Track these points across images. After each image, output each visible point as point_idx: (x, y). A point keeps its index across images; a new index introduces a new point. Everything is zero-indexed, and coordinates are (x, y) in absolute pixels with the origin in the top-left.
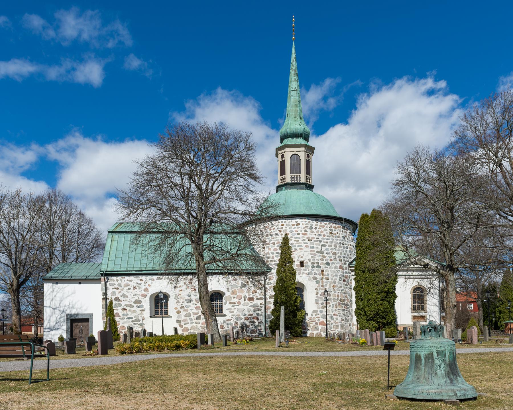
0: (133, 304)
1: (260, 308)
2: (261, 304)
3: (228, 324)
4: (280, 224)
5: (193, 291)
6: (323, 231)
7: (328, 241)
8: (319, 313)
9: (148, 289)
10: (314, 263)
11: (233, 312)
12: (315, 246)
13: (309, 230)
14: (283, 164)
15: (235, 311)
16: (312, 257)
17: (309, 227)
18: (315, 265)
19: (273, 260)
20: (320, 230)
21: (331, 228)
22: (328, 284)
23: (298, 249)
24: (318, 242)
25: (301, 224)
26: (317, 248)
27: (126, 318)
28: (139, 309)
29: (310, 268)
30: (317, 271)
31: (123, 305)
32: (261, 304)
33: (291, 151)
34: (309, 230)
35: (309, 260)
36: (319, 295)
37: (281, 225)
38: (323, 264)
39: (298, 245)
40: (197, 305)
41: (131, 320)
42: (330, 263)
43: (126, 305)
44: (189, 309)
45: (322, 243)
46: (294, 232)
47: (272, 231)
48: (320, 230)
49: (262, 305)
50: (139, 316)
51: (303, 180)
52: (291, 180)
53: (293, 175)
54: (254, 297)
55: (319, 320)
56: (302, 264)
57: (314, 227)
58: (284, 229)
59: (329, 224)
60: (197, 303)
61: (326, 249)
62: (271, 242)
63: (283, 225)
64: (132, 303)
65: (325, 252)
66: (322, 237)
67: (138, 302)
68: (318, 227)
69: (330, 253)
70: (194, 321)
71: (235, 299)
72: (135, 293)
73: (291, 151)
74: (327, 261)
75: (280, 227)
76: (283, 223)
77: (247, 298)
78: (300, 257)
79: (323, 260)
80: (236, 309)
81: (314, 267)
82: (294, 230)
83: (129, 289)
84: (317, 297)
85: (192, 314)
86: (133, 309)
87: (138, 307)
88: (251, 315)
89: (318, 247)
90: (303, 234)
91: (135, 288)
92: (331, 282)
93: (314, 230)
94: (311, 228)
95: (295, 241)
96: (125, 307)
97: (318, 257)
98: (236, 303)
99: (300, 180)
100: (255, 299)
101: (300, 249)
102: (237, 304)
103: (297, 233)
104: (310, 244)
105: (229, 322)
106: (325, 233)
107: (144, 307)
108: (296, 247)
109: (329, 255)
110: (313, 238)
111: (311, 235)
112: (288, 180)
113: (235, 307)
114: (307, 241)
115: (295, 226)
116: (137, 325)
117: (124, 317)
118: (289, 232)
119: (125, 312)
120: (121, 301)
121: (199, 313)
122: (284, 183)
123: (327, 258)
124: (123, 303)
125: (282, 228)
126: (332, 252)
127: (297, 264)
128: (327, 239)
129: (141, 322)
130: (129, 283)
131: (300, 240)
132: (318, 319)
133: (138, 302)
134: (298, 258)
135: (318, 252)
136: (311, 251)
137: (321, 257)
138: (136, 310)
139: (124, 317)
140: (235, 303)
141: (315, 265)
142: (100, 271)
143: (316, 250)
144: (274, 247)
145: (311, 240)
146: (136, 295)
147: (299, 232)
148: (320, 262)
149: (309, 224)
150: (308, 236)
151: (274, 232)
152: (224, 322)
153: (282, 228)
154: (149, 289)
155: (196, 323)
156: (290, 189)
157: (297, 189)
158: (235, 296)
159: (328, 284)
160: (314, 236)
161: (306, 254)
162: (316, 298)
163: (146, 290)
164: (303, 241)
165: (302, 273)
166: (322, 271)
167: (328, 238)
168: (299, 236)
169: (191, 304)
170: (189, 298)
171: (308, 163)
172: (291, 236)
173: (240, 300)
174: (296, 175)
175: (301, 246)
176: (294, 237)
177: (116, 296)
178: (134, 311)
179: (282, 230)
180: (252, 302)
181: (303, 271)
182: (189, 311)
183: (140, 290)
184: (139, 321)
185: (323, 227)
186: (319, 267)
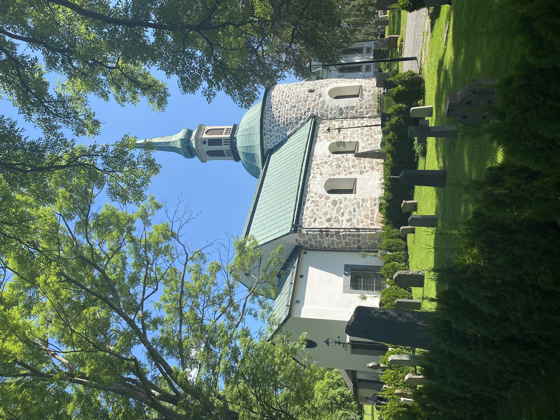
19: (303, 113)
27: (353, 213)
33: (203, 135)
41: (357, 209)
43: (338, 212)
44: (347, 166)
64: (335, 208)
72: (323, 204)
76: (269, 107)
82: (278, 99)
96: (340, 213)
116: (364, 205)
120: (332, 217)
124: (334, 215)
125: (274, 108)
129: (361, 202)
154: (319, 193)
163: (321, 197)
168: (284, 95)
170: (334, 167)
177: (325, 221)
182: (351, 166)
184: (358, 203)
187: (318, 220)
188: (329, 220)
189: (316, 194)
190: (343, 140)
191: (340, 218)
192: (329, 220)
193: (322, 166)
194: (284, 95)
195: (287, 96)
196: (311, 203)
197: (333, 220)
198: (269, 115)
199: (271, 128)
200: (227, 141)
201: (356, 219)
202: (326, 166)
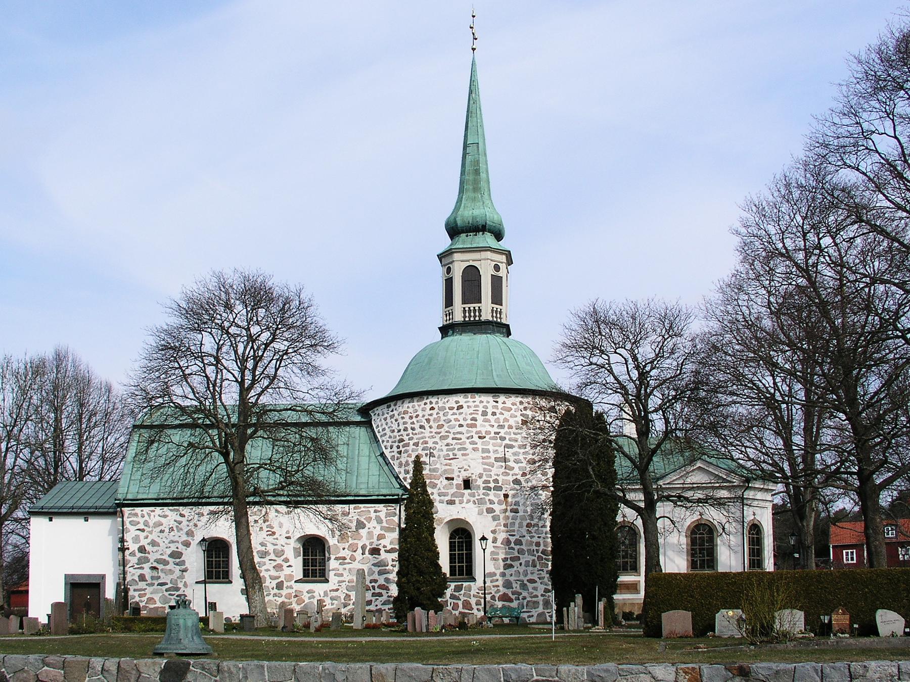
0: (168, 559)
1: (391, 568)
2: (393, 560)
3: (332, 599)
4: (428, 406)
5: (270, 535)
6: (507, 417)
7: (518, 437)
8: (498, 577)
9: (193, 532)
10: (489, 482)
11: (342, 575)
12: (491, 448)
13: (480, 418)
14: (449, 283)
15: (346, 573)
16: (485, 470)
17: (480, 413)
18: (492, 485)
20: (502, 418)
21: (524, 412)
22: (517, 522)
23: (459, 453)
24: (499, 441)
25: (465, 406)
26: (496, 451)
28: (178, 568)
29: (481, 491)
30: (495, 495)
31: (152, 561)
32: (393, 560)
34: (480, 418)
35: (481, 476)
36: (499, 544)
37: (430, 410)
38: (506, 482)
39: (460, 446)
40: (277, 563)
42: (522, 479)
43: (157, 561)
45: (507, 442)
46: (453, 422)
47: (414, 420)
48: (502, 418)
49: (394, 563)
50: (179, 581)
51: (486, 316)
52: (465, 317)
54: (380, 547)
55: (498, 591)
56: (467, 484)
57: (490, 411)
58: (435, 416)
59: (521, 403)
60: (276, 558)
61: (515, 454)
62: (411, 442)
63: (432, 409)
64: (166, 557)
65: (512, 458)
66: (506, 429)
67: (176, 555)
68: (498, 412)
69: (523, 460)
70: (273, 592)
71: (346, 550)
74: (515, 477)
75: (428, 412)
77: (368, 548)
78: (462, 470)
79: (508, 474)
80: (347, 571)
81: (489, 489)
82: (452, 418)
83: (162, 531)
84: (494, 547)
85: (268, 578)
86: (168, 567)
87: (177, 564)
88: (376, 581)
89: (497, 450)
90: (468, 425)
91: (171, 529)
92: (523, 518)
93: (489, 416)
94: (484, 413)
95: (453, 439)
96: (155, 564)
97: (497, 470)
98: (348, 558)
99: (480, 316)
100: (382, 552)
101: (463, 455)
102: (348, 561)
103: (458, 423)
104: (483, 443)
105: (334, 594)
106: (512, 422)
107: (187, 565)
108: (456, 452)
109: (520, 465)
110: (488, 433)
111: (484, 426)
112: (458, 317)
113: (345, 566)
114: (476, 439)
115: (455, 411)
116: (175, 597)
117: (153, 582)
118: (443, 423)
119: (155, 574)
120: (149, 553)
121: (280, 577)
122: (451, 321)
123: (516, 470)
124: (152, 557)
125: (431, 415)
126: (525, 458)
127: (456, 485)
128: (514, 434)
130: (162, 520)
131: (463, 437)
132: (496, 589)
133: (176, 555)
134: (460, 472)
135: (496, 459)
136: (483, 458)
137: (503, 470)
138: (173, 569)
139: (153, 582)
140: (344, 558)
141: (492, 485)
142: (116, 500)
143: (493, 456)
144: (417, 450)
145: (485, 437)
146: (172, 542)
147: (462, 422)
148: (500, 478)
149: (481, 405)
150: (478, 429)
151: (417, 421)
152: (326, 594)
153: (431, 415)
155: (275, 595)
156: (461, 334)
157: (474, 334)
158: (347, 545)
159: (517, 522)
160: (490, 429)
161: (472, 464)
162: (493, 549)
164: (468, 438)
165: (465, 501)
166: (506, 496)
167: (517, 431)
168: (460, 429)
169: (266, 560)
170: (263, 548)
171: (497, 282)
172: (447, 429)
173: (354, 553)
175: (465, 449)
176: (452, 431)
177: (140, 544)
178: (171, 572)
179: (431, 418)
180: (376, 556)
181: (469, 497)
183: (179, 534)
184: (178, 589)
185: (509, 410)
186: (499, 488)
187: (142, 535)
188: (142, 549)
189: (196, 525)
190: (333, 557)
191: (147, 566)
192: (142, 549)
193: (261, 529)
194: (460, 429)
195: (458, 436)
196: (175, 521)
197: (143, 555)
198: (417, 407)
199: (396, 416)
200: (477, 314)
201: (146, 587)
202: (264, 534)
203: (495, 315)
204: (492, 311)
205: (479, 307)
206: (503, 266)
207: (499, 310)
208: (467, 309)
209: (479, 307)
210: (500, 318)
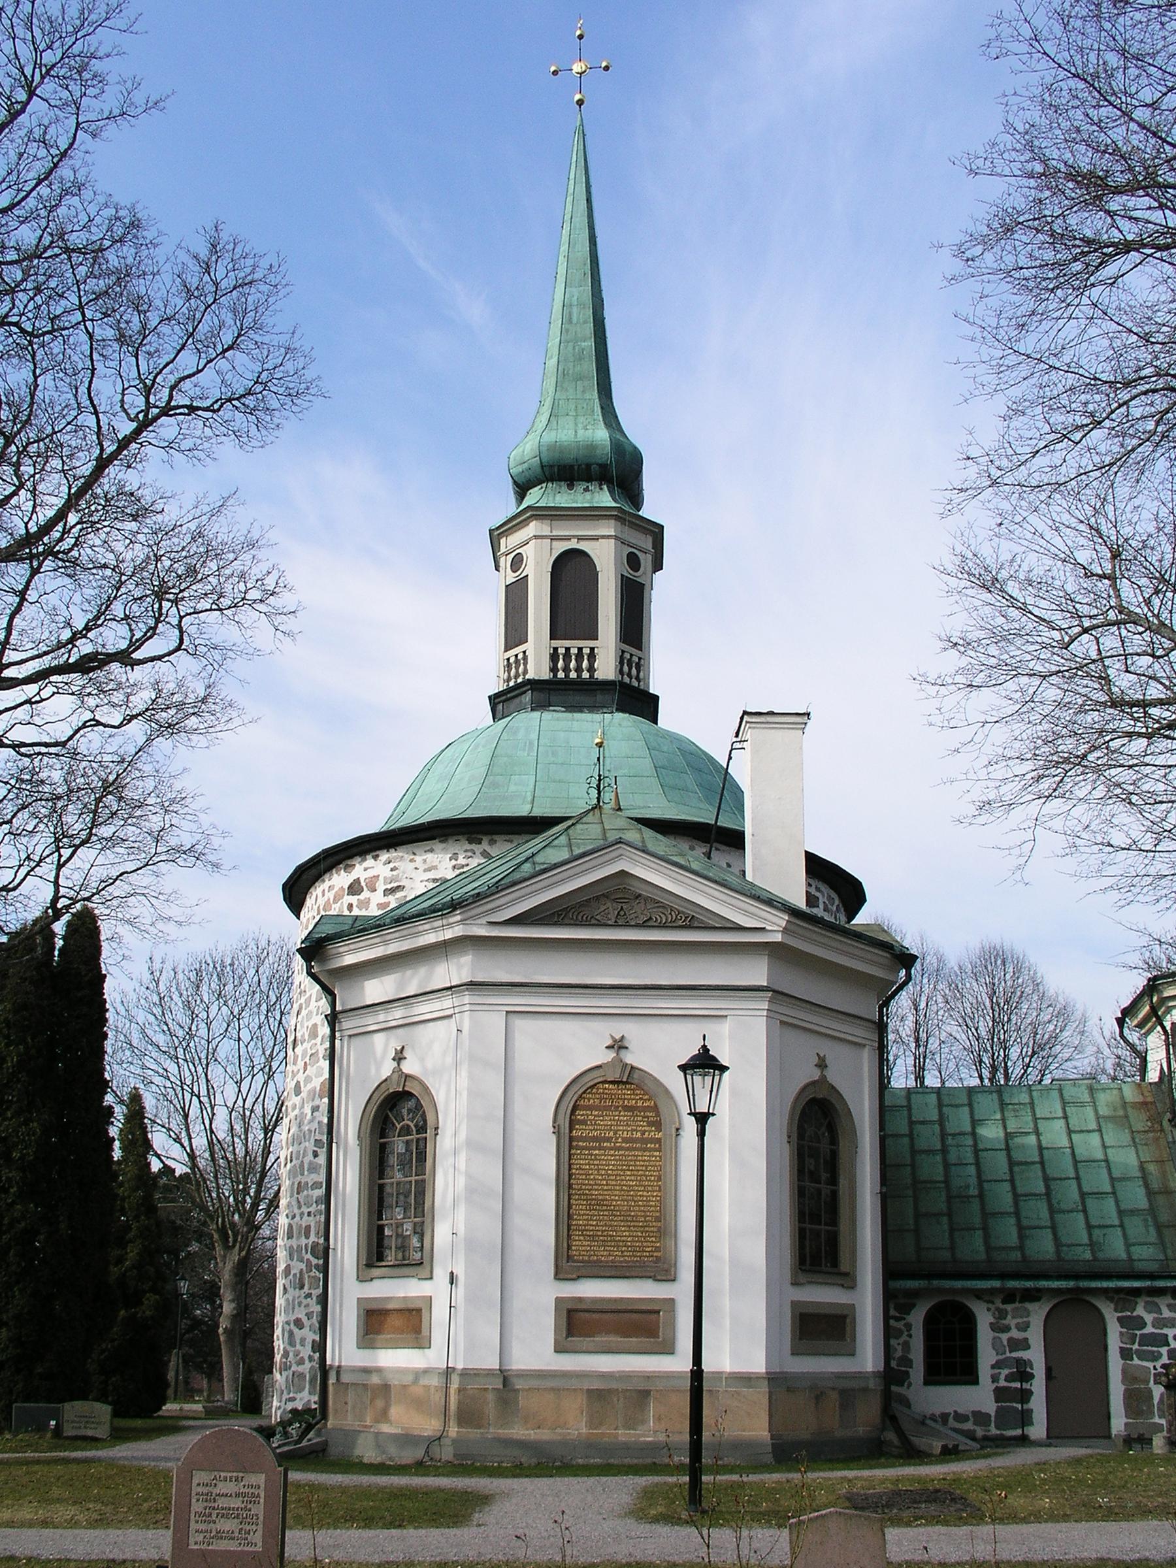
51: (606, 668)
52: (554, 670)
53: (562, 645)
73: (553, 539)
99: (591, 669)
112: (537, 669)
122: (520, 680)
174: (574, 645)
203: (626, 668)
204: (622, 658)
205: (592, 649)
206: (646, 561)
207: (635, 659)
208: (562, 651)
209: (592, 649)
210: (638, 679)
